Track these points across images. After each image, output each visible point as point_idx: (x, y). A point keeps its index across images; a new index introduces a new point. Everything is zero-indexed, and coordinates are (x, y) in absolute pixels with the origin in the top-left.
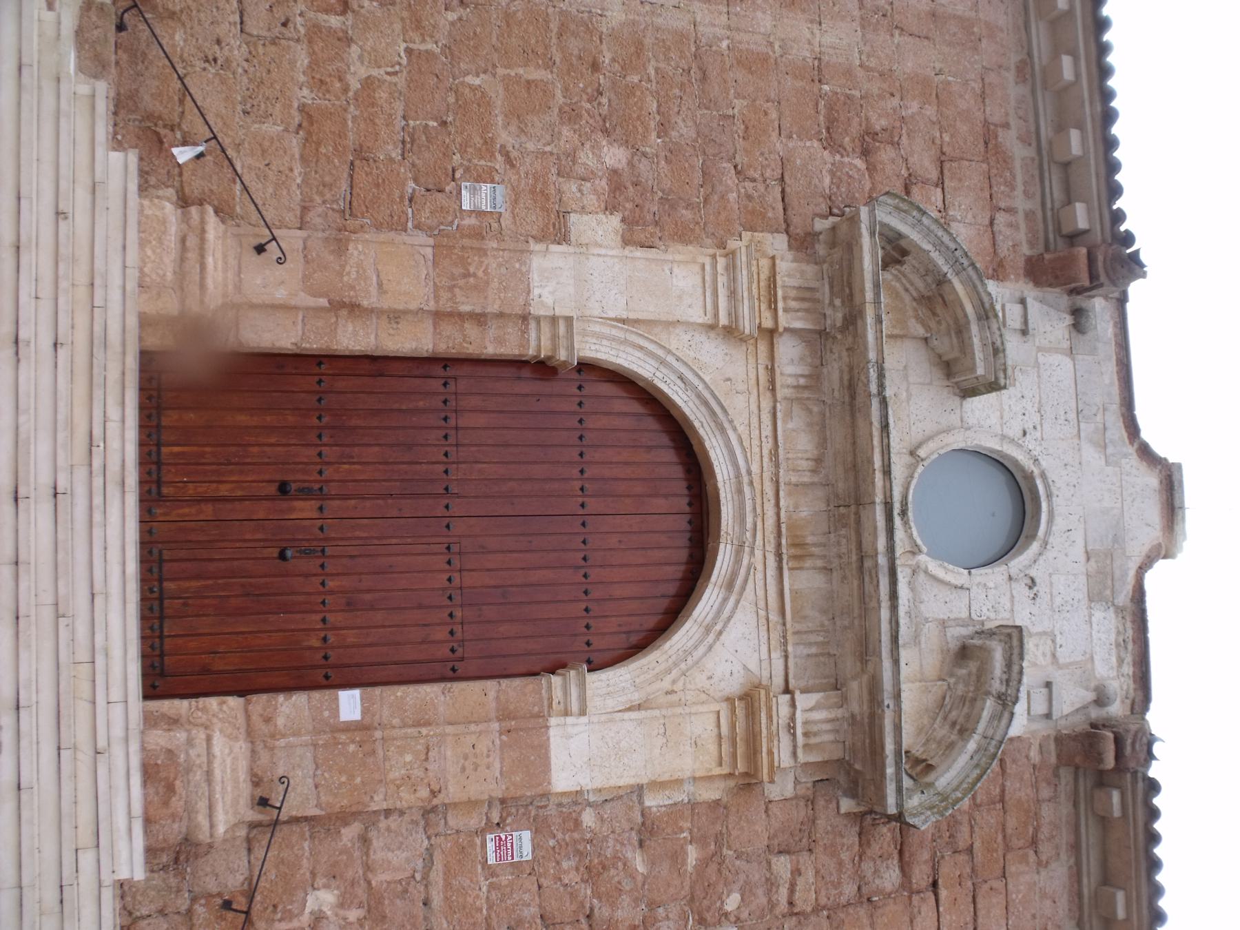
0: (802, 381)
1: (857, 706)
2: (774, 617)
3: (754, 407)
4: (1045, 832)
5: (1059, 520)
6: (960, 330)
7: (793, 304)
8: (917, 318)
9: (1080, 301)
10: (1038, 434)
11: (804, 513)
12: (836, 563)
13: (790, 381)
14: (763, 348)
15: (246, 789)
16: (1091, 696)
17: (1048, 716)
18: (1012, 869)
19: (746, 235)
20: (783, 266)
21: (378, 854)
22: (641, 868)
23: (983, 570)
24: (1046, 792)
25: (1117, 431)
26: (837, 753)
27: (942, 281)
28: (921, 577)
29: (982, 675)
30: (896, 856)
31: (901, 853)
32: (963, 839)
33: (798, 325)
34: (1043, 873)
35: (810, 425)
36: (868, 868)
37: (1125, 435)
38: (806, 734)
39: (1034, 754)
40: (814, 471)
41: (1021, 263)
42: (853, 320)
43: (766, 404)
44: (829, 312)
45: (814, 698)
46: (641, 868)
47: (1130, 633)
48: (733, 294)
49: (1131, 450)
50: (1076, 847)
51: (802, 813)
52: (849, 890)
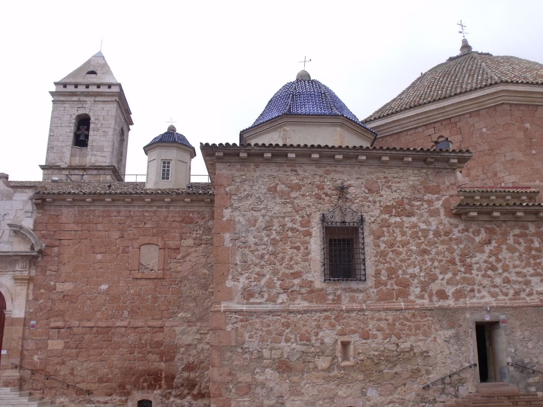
1: (19, 258)
4: (56, 213)
16: (30, 202)
17: (32, 212)
18: (61, 221)
21: (30, 348)
22: (42, 301)
24: (48, 213)
26: (28, 261)
32: (52, 233)
36: (53, 255)
39: (39, 215)
45: (17, 266)
46: (42, 301)
47: (20, 190)
50: (61, 206)
51: (39, 269)
52: (56, 259)
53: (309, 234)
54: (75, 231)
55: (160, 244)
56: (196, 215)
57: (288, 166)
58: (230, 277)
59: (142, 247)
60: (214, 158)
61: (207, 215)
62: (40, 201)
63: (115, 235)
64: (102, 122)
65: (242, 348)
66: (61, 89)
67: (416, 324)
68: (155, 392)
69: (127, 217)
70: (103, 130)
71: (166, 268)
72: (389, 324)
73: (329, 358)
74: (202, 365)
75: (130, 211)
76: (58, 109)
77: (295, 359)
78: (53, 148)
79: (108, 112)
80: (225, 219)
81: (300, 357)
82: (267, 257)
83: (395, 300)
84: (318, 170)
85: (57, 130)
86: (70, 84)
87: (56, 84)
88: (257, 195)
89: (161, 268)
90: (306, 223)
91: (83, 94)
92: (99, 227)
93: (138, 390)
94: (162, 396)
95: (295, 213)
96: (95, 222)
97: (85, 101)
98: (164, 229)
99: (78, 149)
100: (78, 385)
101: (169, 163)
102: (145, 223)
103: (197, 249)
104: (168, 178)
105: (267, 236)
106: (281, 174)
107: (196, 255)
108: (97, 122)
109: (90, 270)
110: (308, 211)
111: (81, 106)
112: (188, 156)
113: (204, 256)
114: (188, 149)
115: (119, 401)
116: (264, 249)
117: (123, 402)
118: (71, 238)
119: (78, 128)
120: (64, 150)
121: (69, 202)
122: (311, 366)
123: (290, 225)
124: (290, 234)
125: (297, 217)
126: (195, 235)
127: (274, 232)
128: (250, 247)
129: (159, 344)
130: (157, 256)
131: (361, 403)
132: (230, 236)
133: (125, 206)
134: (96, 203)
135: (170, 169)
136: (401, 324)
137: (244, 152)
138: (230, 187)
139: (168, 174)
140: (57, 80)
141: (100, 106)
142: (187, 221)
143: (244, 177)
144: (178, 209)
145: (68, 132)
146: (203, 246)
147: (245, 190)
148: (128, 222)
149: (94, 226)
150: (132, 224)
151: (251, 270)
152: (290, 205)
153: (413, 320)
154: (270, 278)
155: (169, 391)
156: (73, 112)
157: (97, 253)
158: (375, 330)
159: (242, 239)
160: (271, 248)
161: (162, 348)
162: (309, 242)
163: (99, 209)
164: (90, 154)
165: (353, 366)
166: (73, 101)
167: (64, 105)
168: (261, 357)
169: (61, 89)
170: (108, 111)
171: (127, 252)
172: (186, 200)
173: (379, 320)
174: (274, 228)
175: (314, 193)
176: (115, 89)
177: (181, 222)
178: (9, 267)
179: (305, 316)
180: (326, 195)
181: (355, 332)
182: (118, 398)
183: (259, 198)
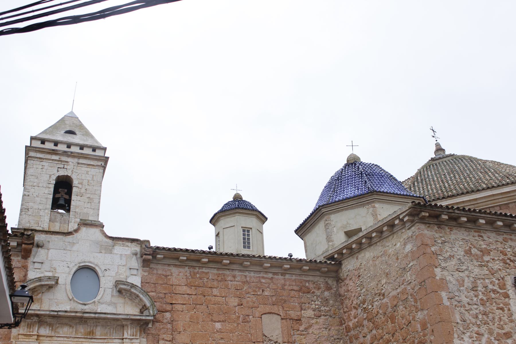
0: (51, 329)
2: (106, 341)
3: (56, 342)
4: (164, 273)
5: (92, 260)
6: (42, 286)
7: (31, 330)
8: (37, 295)
9: (35, 244)
10: (69, 263)
11: (82, 331)
12: (95, 324)
13: (50, 332)
14: (41, 338)
16: (134, 257)
19: (12, 340)
20: (21, 332)
23: (101, 282)
24: (155, 272)
25: (69, 238)
26: (138, 328)
28: (101, 301)
29: (125, 290)
30: (163, 313)
31: (163, 312)
32: (162, 295)
33: (37, 329)
34: (173, 275)
35: (61, 327)
36: (165, 321)
37: (71, 236)
38: (133, 336)
39: (146, 274)
40: (73, 327)
41: (23, 260)
42: (37, 315)
43: (55, 338)
44: (34, 320)
45: (125, 333)
47: (121, 242)
49: (76, 235)
50: (169, 265)
51: (150, 337)
52: (169, 326)
53: (507, 296)
54: (188, 294)
55: (281, 314)
56: (311, 286)
57: (475, 231)
58: (456, 336)
59: (263, 316)
60: (416, 218)
61: (322, 286)
63: (233, 302)
64: (87, 187)
66: (37, 144)
69: (244, 283)
70: (88, 196)
71: (290, 340)
75: (246, 276)
76: (34, 166)
78: (28, 209)
79: (93, 177)
80: (438, 278)
82: (480, 316)
84: (498, 237)
85: (33, 190)
86: (50, 141)
87: (32, 138)
88: (458, 257)
89: (286, 340)
90: (503, 286)
91: (65, 153)
92: (215, 292)
95: (491, 276)
96: (209, 286)
97: (67, 162)
98: (283, 298)
101: (248, 231)
102: (263, 291)
103: (318, 320)
105: (476, 296)
106: (470, 238)
107: (318, 327)
108: (80, 186)
109: (209, 340)
110: (503, 274)
111: (62, 166)
113: (326, 328)
116: (476, 309)
118: (185, 302)
119: (56, 190)
120: (41, 213)
123: (490, 287)
124: (493, 296)
125: (494, 279)
126: (314, 306)
127: (480, 293)
128: (465, 306)
130: (279, 327)
132: (446, 295)
133: (240, 271)
134: (211, 265)
135: (251, 237)
137: (445, 215)
138: (434, 247)
139: (249, 243)
140: (34, 135)
141: (84, 169)
142: (304, 290)
143: (443, 239)
144: (294, 277)
145: (46, 193)
146: (322, 317)
147: (447, 251)
148: (245, 288)
149: (209, 290)
150: (250, 290)
151: (471, 330)
152: (485, 268)
154: (489, 338)
156: (49, 173)
157: (215, 322)
159: (457, 298)
160: (482, 308)
162: (510, 304)
163: (213, 272)
164: (73, 221)
166: (53, 160)
169: (37, 144)
170: (93, 176)
171: (248, 322)
172: (305, 268)
174: (479, 289)
175: (501, 258)
176: (98, 153)
177: (299, 291)
178: (114, 334)
180: (511, 261)
183: (459, 259)
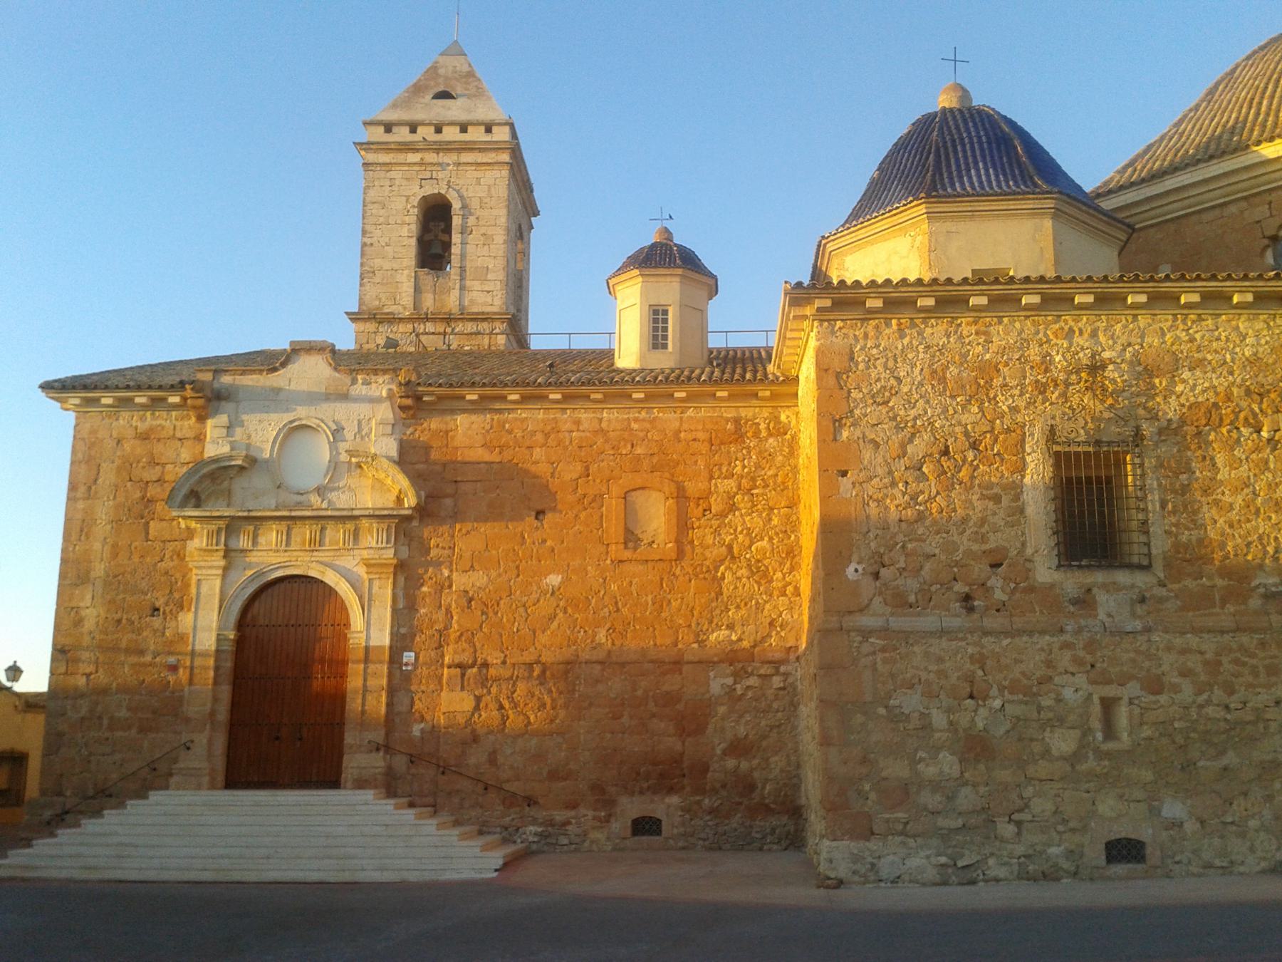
14: (233, 554)
15: (374, 754)
27: (205, 476)
36: (443, 514)
41: (198, 425)
48: (210, 567)
62: (409, 402)
65: (886, 707)
67: (1267, 662)
68: (667, 800)
70: (483, 230)
72: (1206, 663)
73: (1078, 733)
74: (764, 743)
77: (1002, 731)
81: (1013, 728)
83: (1217, 610)
87: (367, 124)
93: (632, 794)
94: (683, 809)
96: (528, 443)
99: (427, 277)
100: (507, 786)
104: (665, 346)
112: (705, 294)
114: (704, 279)
115: (594, 818)
117: (600, 821)
120: (399, 277)
121: (471, 402)
122: (1037, 748)
129: (670, 699)
131: (1150, 831)
136: (1236, 662)
141: (471, 174)
153: (1261, 654)
155: (698, 798)
158: (1175, 674)
161: (680, 707)
165: (1128, 752)
167: (392, 174)
168: (926, 727)
173: (1183, 652)
176: (501, 134)
179: (1017, 640)
181: (1132, 677)
182: (590, 813)
